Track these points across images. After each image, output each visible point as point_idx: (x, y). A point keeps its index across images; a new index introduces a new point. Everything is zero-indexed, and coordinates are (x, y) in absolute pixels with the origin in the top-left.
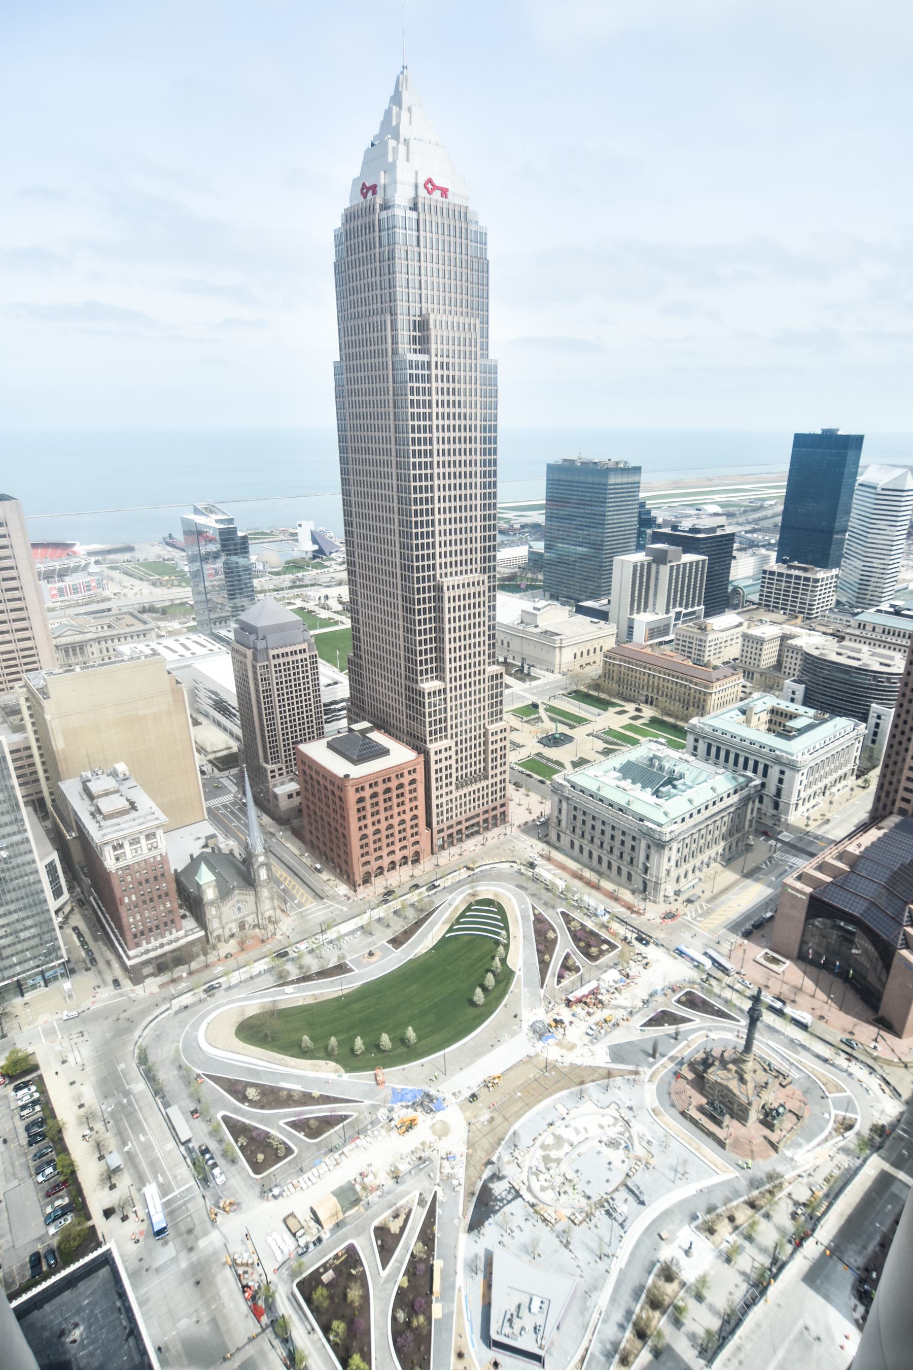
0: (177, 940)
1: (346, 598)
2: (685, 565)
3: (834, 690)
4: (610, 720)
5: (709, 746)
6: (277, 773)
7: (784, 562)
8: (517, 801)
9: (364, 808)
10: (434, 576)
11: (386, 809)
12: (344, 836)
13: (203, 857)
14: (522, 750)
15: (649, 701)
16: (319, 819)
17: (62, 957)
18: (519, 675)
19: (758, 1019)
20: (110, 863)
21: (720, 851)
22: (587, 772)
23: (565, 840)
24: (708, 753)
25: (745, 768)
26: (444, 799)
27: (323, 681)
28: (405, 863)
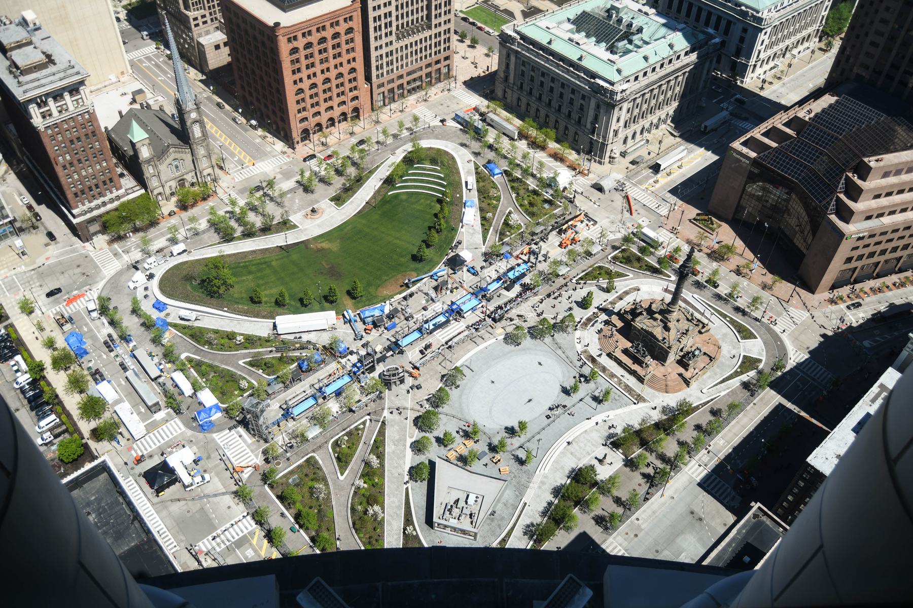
0: (118, 198)
6: (200, 21)
8: (462, 53)
9: (298, 61)
11: (322, 62)
12: (278, 90)
13: (131, 114)
17: (7, 216)
20: (37, 120)
21: (671, 113)
26: (384, 51)
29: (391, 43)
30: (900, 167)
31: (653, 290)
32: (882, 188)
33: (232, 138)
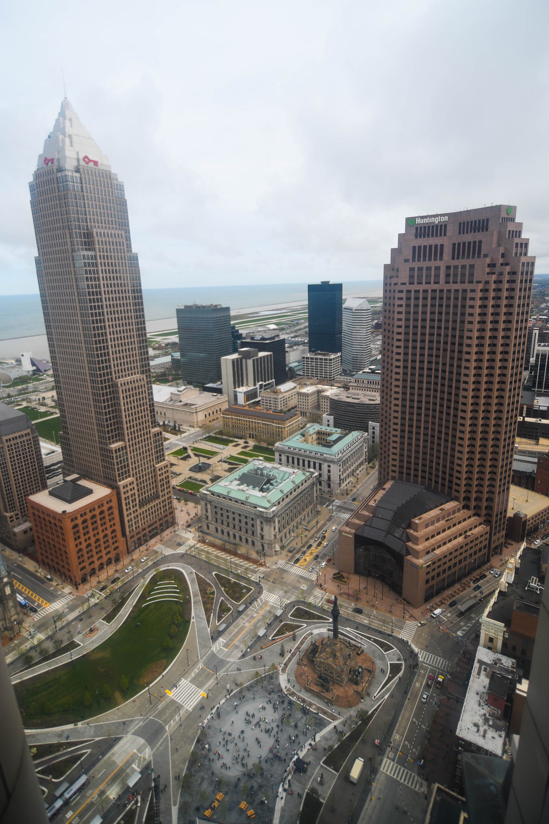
1: (56, 398)
2: (261, 358)
3: (349, 417)
4: (231, 451)
5: (288, 457)
7: (313, 352)
8: (180, 509)
9: (78, 532)
10: (112, 378)
12: (66, 552)
14: (181, 476)
15: (251, 436)
16: (47, 544)
18: (173, 431)
19: (338, 616)
22: (220, 484)
23: (212, 528)
24: (288, 462)
25: (309, 467)
26: (132, 516)
27: (43, 451)
28: (110, 563)
29: (137, 510)
30: (433, 520)
31: (321, 630)
32: (428, 534)
33: (34, 590)
